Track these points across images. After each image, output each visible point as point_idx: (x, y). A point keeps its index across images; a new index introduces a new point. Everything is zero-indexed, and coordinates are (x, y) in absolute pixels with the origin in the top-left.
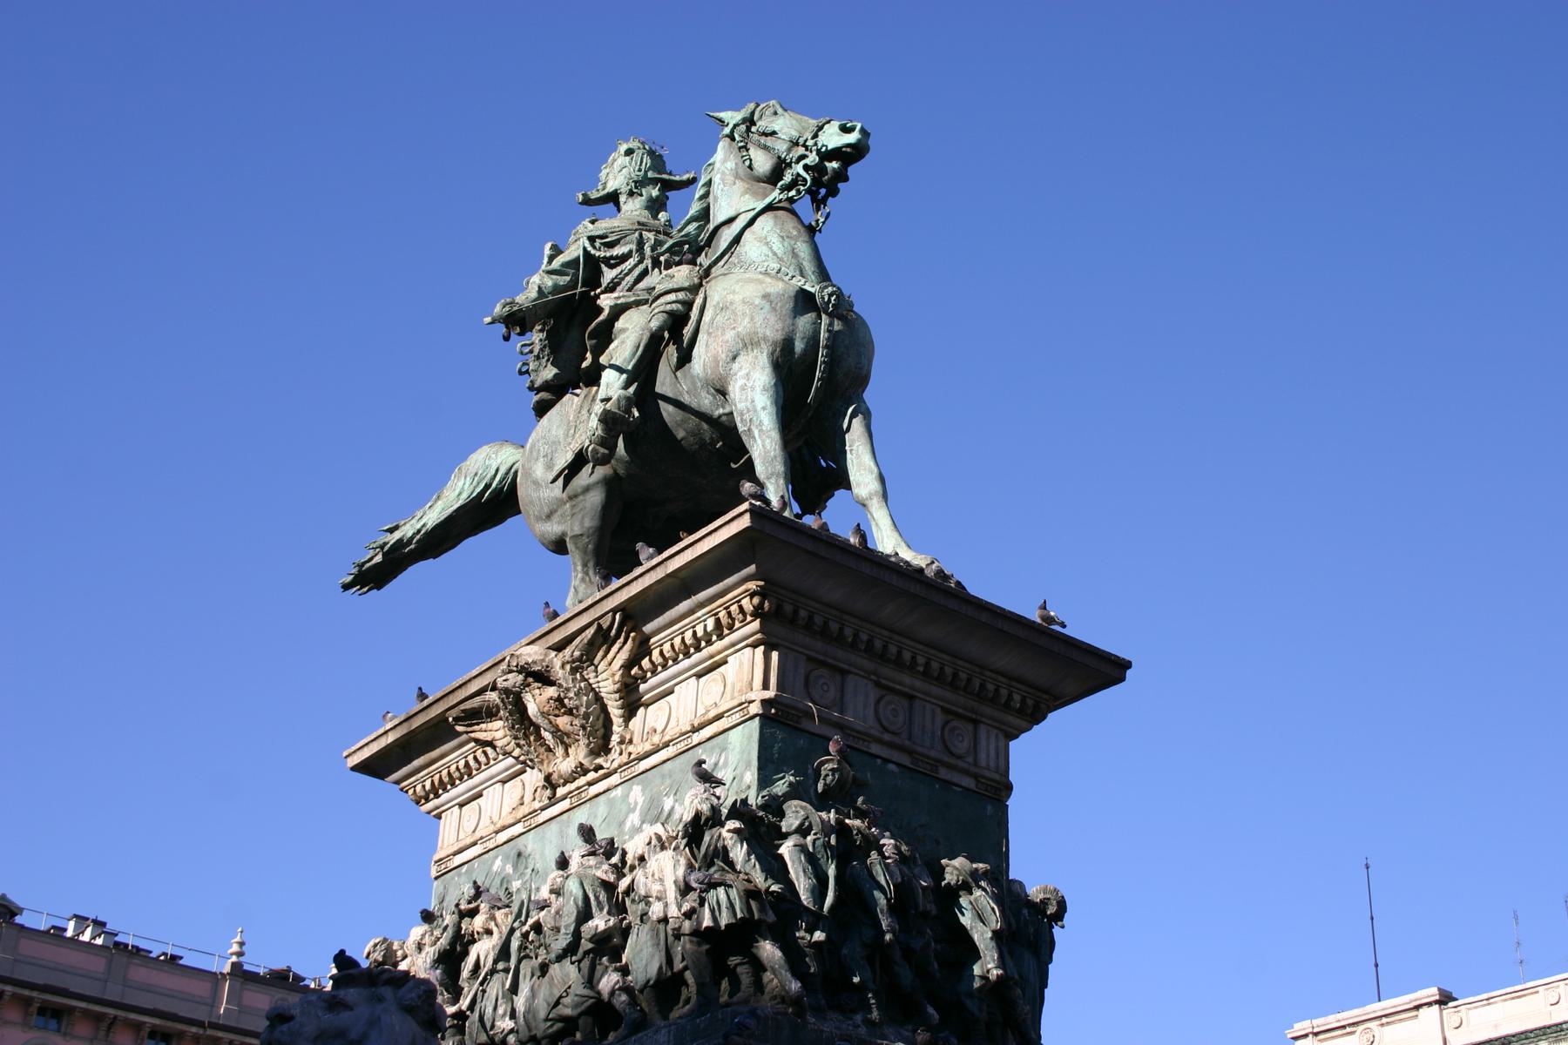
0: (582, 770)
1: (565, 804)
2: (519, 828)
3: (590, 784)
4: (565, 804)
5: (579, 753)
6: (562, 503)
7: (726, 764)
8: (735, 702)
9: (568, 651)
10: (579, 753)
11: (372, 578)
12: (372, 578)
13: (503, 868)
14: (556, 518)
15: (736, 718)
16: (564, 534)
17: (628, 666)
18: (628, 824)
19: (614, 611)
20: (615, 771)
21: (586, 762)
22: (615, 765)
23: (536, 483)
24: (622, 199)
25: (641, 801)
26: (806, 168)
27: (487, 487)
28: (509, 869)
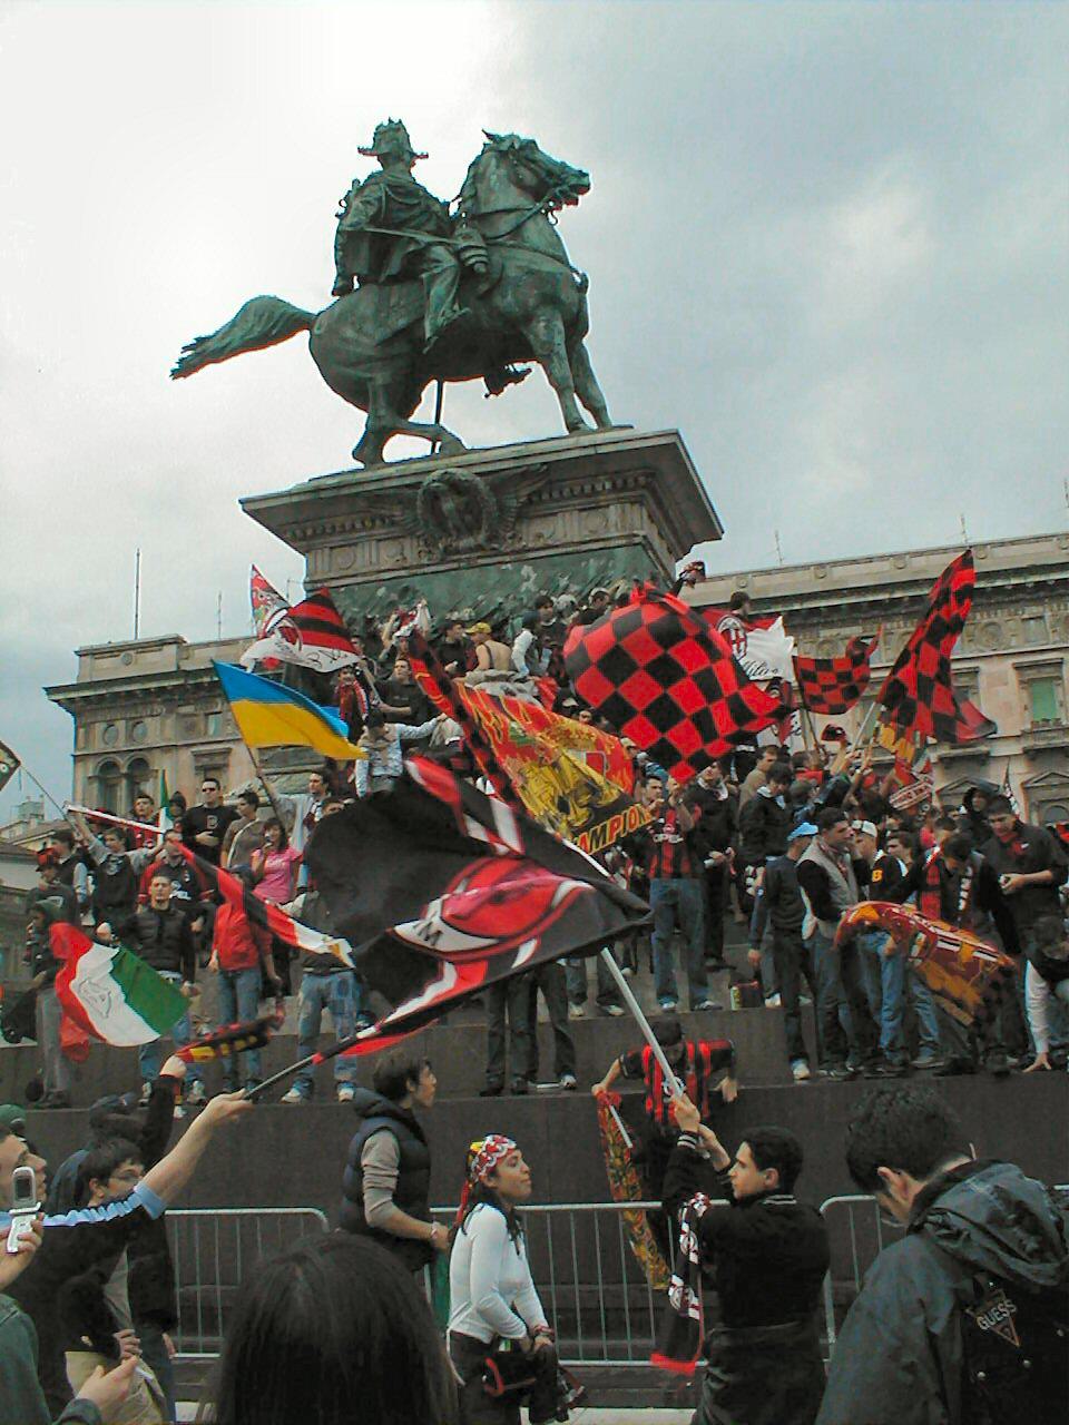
0: (479, 547)
1: (455, 565)
2: (403, 573)
3: (479, 557)
4: (455, 565)
5: (481, 537)
6: (370, 359)
7: (614, 567)
8: (627, 533)
10: (481, 537)
11: (184, 369)
12: (184, 369)
13: (388, 596)
15: (624, 542)
16: (371, 379)
18: (523, 589)
20: (507, 554)
21: (484, 544)
22: (508, 550)
23: (346, 340)
24: (390, 161)
25: (533, 576)
26: (560, 192)
27: (273, 327)
28: (394, 596)
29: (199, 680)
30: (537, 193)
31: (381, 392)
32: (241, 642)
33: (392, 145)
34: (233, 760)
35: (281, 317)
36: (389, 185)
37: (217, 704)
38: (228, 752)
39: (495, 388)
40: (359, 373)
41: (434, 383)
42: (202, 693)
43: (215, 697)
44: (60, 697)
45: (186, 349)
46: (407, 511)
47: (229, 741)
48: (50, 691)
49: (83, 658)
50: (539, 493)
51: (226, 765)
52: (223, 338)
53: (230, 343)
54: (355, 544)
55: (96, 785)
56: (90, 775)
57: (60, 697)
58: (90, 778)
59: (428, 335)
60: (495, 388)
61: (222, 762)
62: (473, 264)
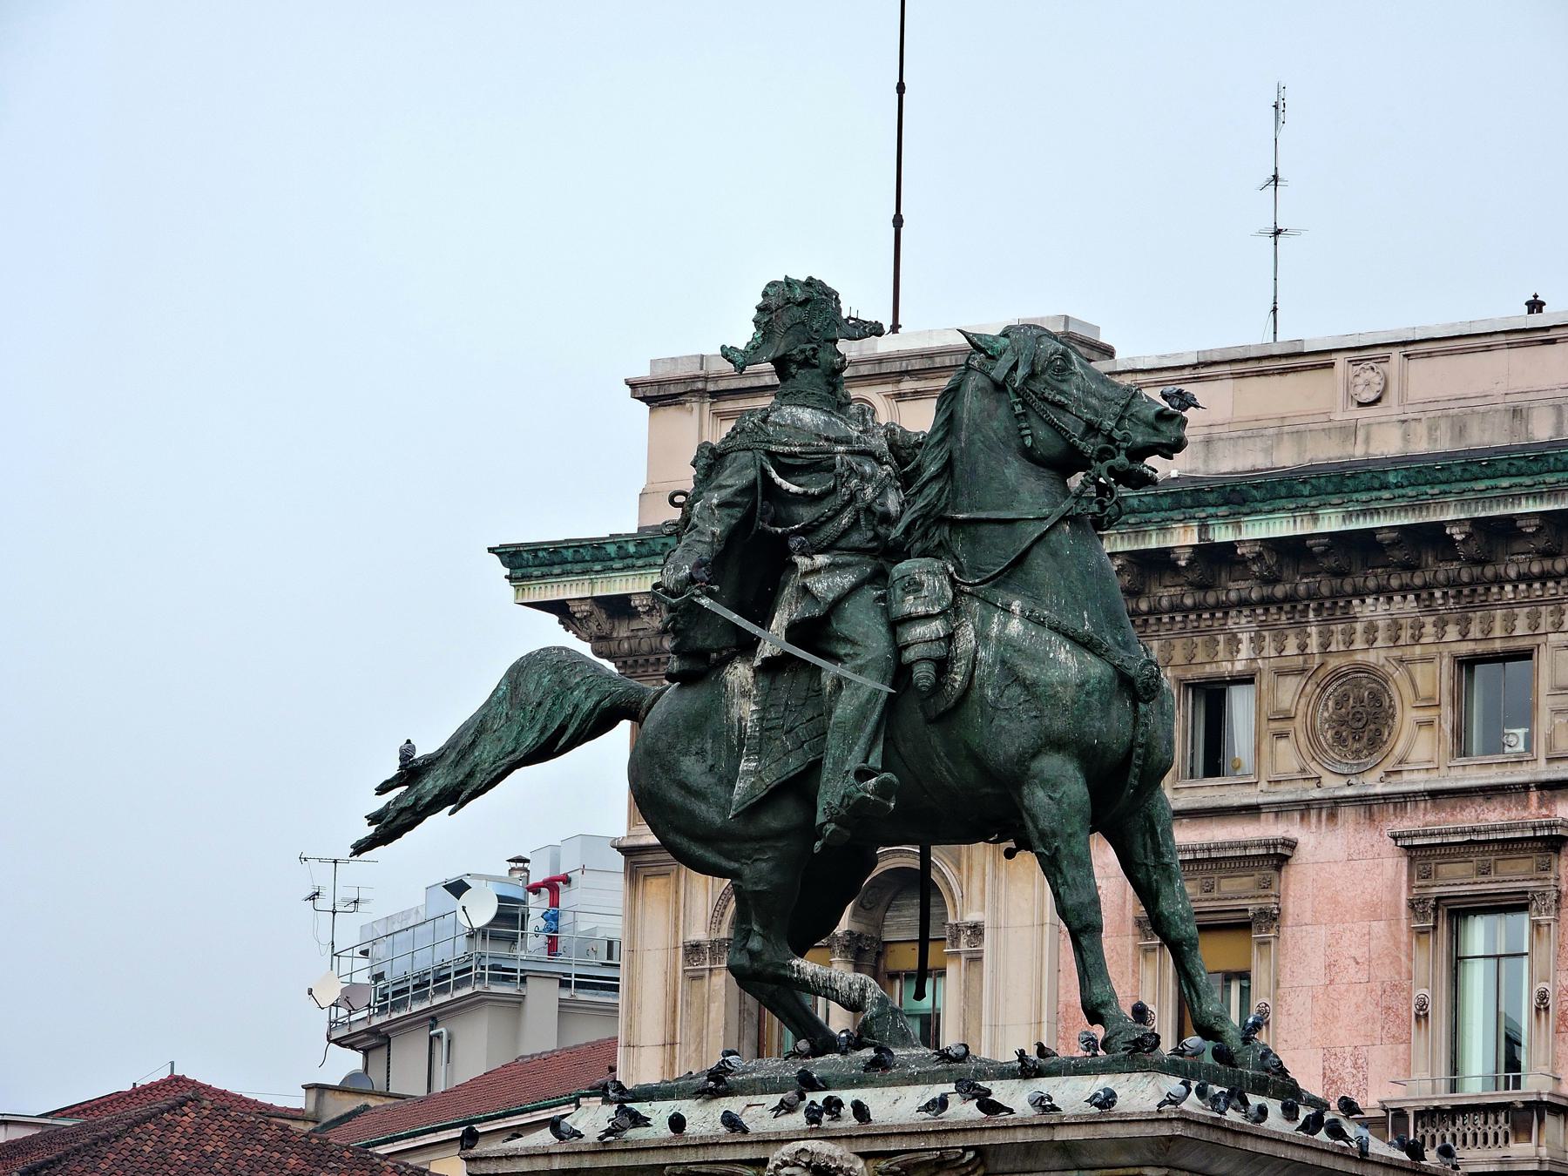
29: (1153, 542)
32: (1340, 360)
33: (801, 327)
34: (1299, 890)
37: (1233, 640)
38: (1279, 857)
42: (1165, 594)
43: (1225, 607)
44: (571, 590)
45: (383, 789)
47: (1280, 810)
48: (524, 562)
49: (670, 414)
51: (1271, 918)
52: (457, 763)
53: (471, 775)
55: (720, 983)
56: (699, 934)
57: (571, 590)
58: (694, 950)
59: (820, 819)
61: (1253, 906)
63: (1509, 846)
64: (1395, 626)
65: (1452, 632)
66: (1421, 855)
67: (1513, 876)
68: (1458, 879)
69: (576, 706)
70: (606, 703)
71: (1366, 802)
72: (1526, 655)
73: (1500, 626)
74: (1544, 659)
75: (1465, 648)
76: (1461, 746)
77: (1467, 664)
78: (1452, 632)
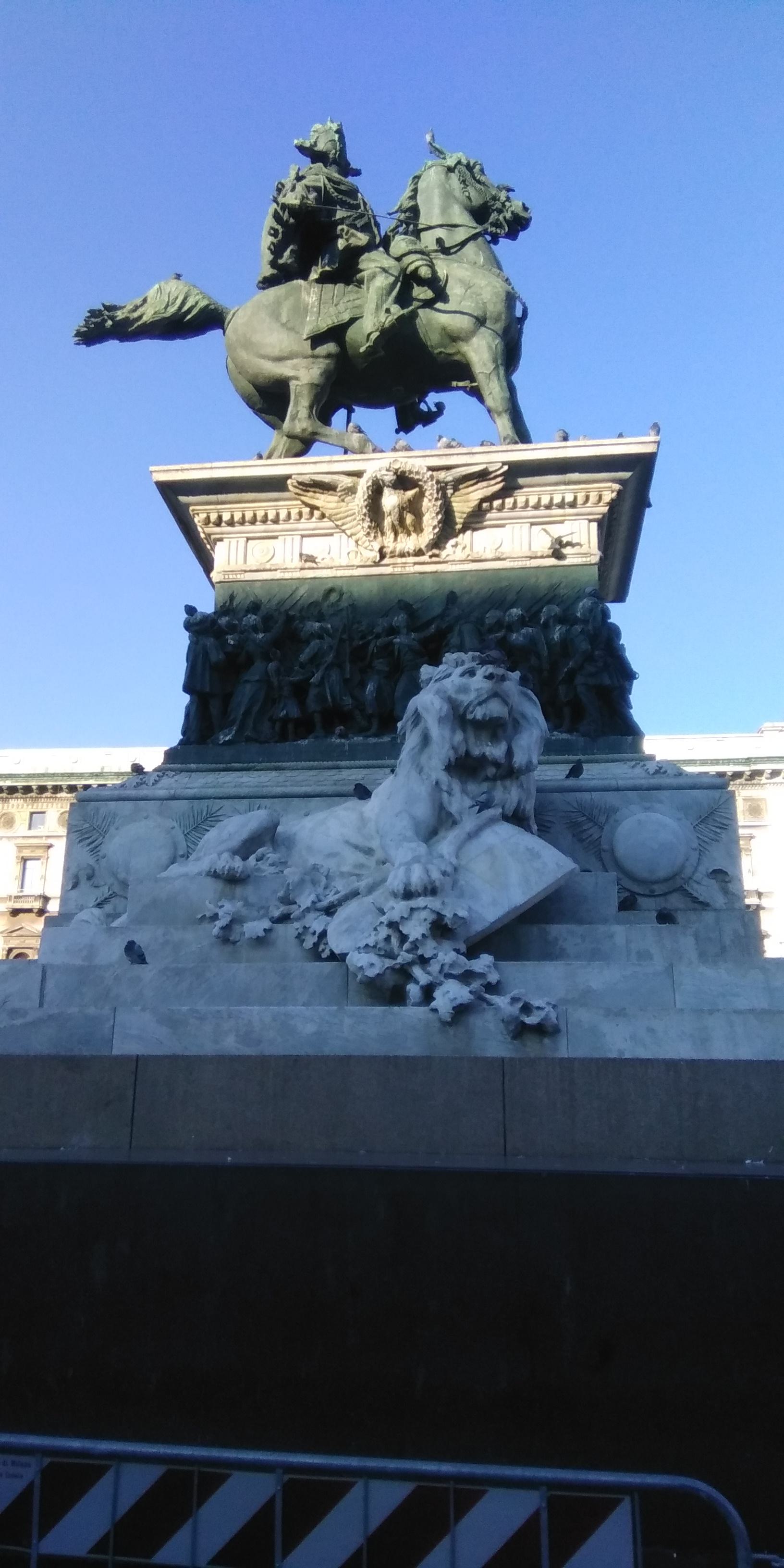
9: (442, 475)
14: (289, 363)
17: (483, 500)
19: (504, 463)
26: (505, 218)
30: (480, 213)
31: (305, 392)
35: (197, 303)
36: (327, 178)
39: (405, 425)
40: (283, 370)
41: (342, 413)
46: (342, 504)
50: (490, 499)
53: (140, 317)
54: (275, 537)
60: (405, 425)
62: (417, 269)
63: (38, 847)
64: (18, 805)
65: (30, 807)
66: (20, 848)
67: (38, 853)
68: (26, 853)
69: (197, 303)
70: (212, 307)
71: (8, 838)
72: (44, 813)
73: (40, 806)
74: (47, 814)
75: (32, 810)
76: (30, 828)
77: (32, 814)
78: (30, 807)
